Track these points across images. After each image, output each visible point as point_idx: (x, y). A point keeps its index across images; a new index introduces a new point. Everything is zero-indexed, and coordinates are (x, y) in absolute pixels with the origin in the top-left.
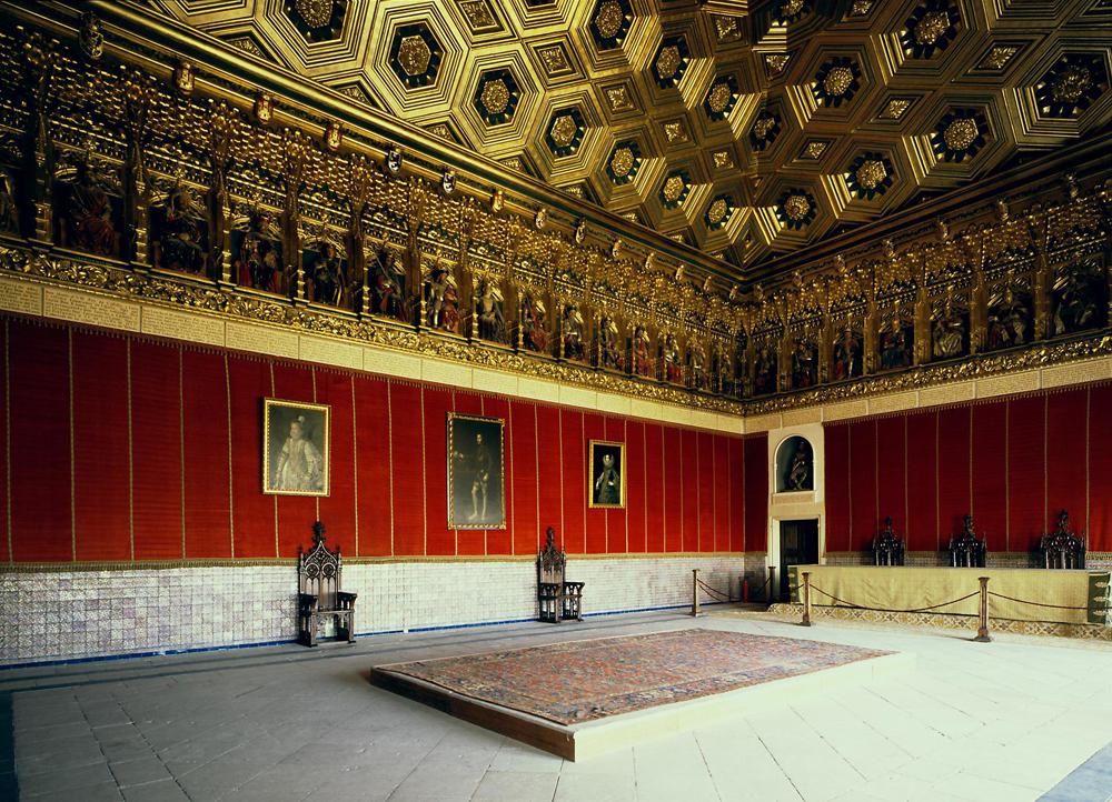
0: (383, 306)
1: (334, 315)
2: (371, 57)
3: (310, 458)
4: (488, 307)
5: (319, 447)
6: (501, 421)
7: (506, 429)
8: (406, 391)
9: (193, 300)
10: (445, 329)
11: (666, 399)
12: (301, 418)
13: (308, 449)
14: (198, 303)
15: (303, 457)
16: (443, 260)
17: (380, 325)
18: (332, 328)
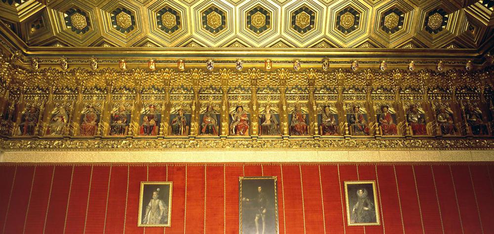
0: (203, 131)
1: (178, 139)
2: (193, 29)
3: (161, 208)
4: (268, 117)
5: (166, 203)
6: (275, 178)
7: (279, 182)
8: (215, 169)
9: (185, 145)
10: (240, 134)
11: (412, 147)
12: (158, 189)
13: (161, 204)
14: (254, 146)
15: (158, 207)
16: (242, 102)
17: (201, 139)
18: (244, 145)
